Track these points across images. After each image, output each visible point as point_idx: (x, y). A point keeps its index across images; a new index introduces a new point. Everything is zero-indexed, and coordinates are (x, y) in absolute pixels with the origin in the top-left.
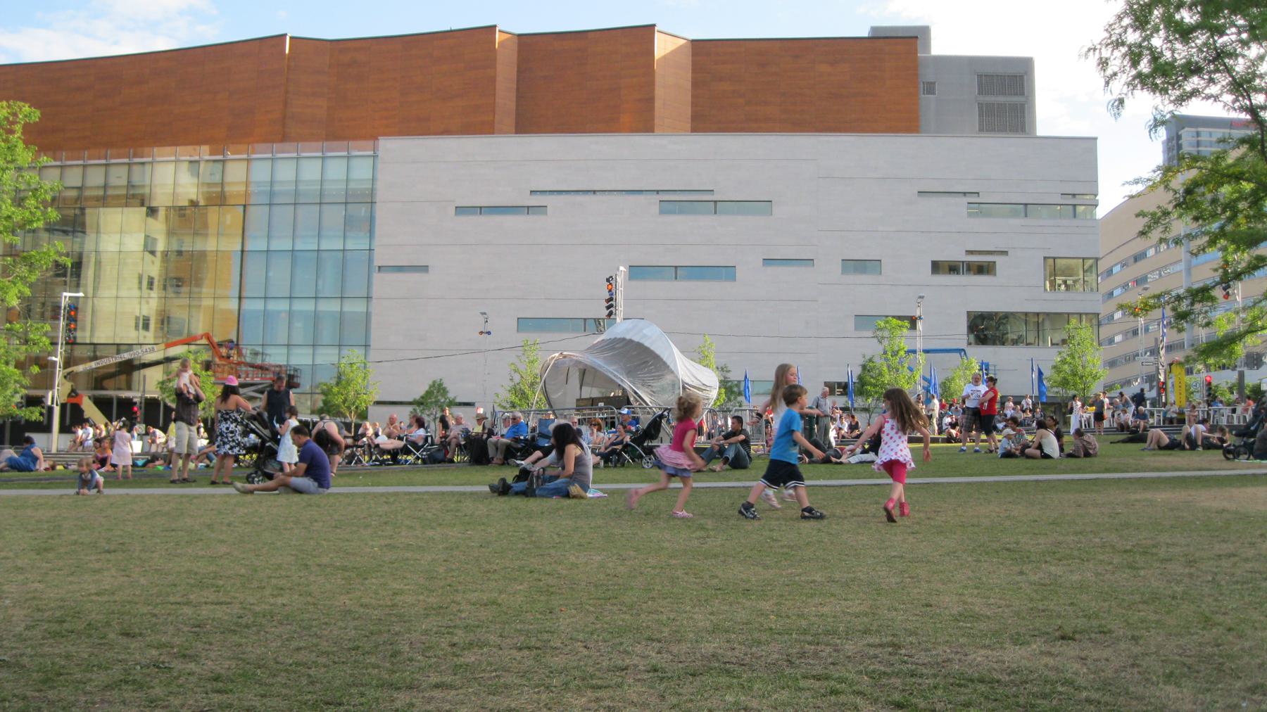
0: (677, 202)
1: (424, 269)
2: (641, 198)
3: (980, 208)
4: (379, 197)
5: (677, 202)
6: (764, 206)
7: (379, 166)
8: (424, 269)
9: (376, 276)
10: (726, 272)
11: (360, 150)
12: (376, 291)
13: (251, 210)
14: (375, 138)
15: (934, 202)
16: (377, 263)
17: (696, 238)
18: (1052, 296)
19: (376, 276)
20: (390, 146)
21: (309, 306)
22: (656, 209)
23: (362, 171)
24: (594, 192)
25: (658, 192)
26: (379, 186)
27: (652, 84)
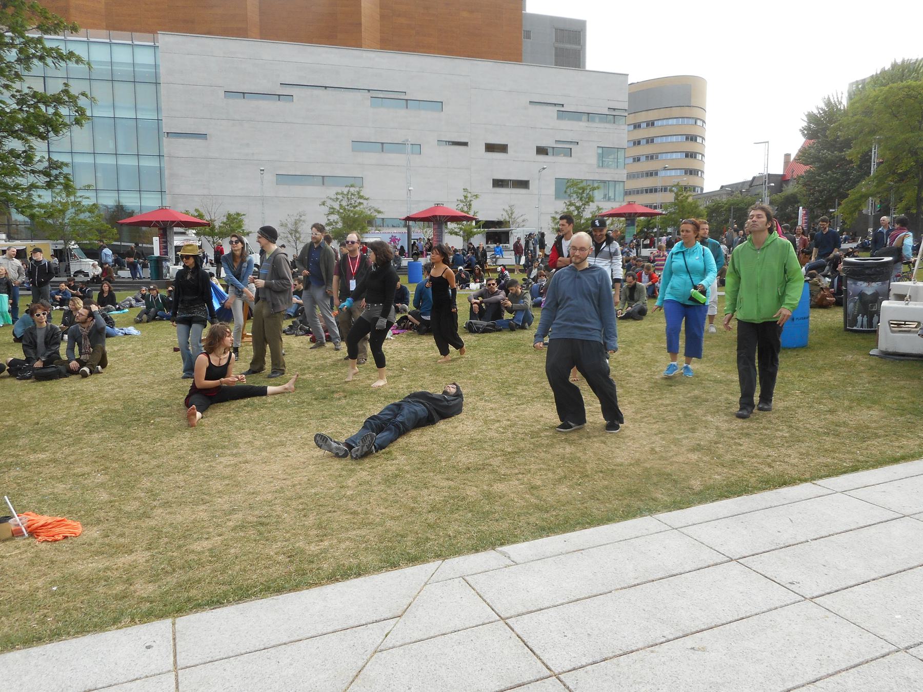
0: (382, 97)
1: (203, 136)
2: (358, 95)
3: (563, 114)
4: (162, 80)
5: (382, 97)
6: (439, 105)
7: (159, 54)
8: (203, 136)
9: (165, 140)
10: (417, 148)
11: (143, 40)
12: (165, 151)
13: (48, 80)
14: (154, 32)
15: (539, 108)
16: (165, 129)
17: (394, 123)
18: (601, 170)
19: (165, 140)
20: (166, 40)
21: (111, 161)
22: (368, 102)
23: (144, 57)
24: (326, 87)
25: (369, 90)
26: (162, 70)
27: (359, 13)
